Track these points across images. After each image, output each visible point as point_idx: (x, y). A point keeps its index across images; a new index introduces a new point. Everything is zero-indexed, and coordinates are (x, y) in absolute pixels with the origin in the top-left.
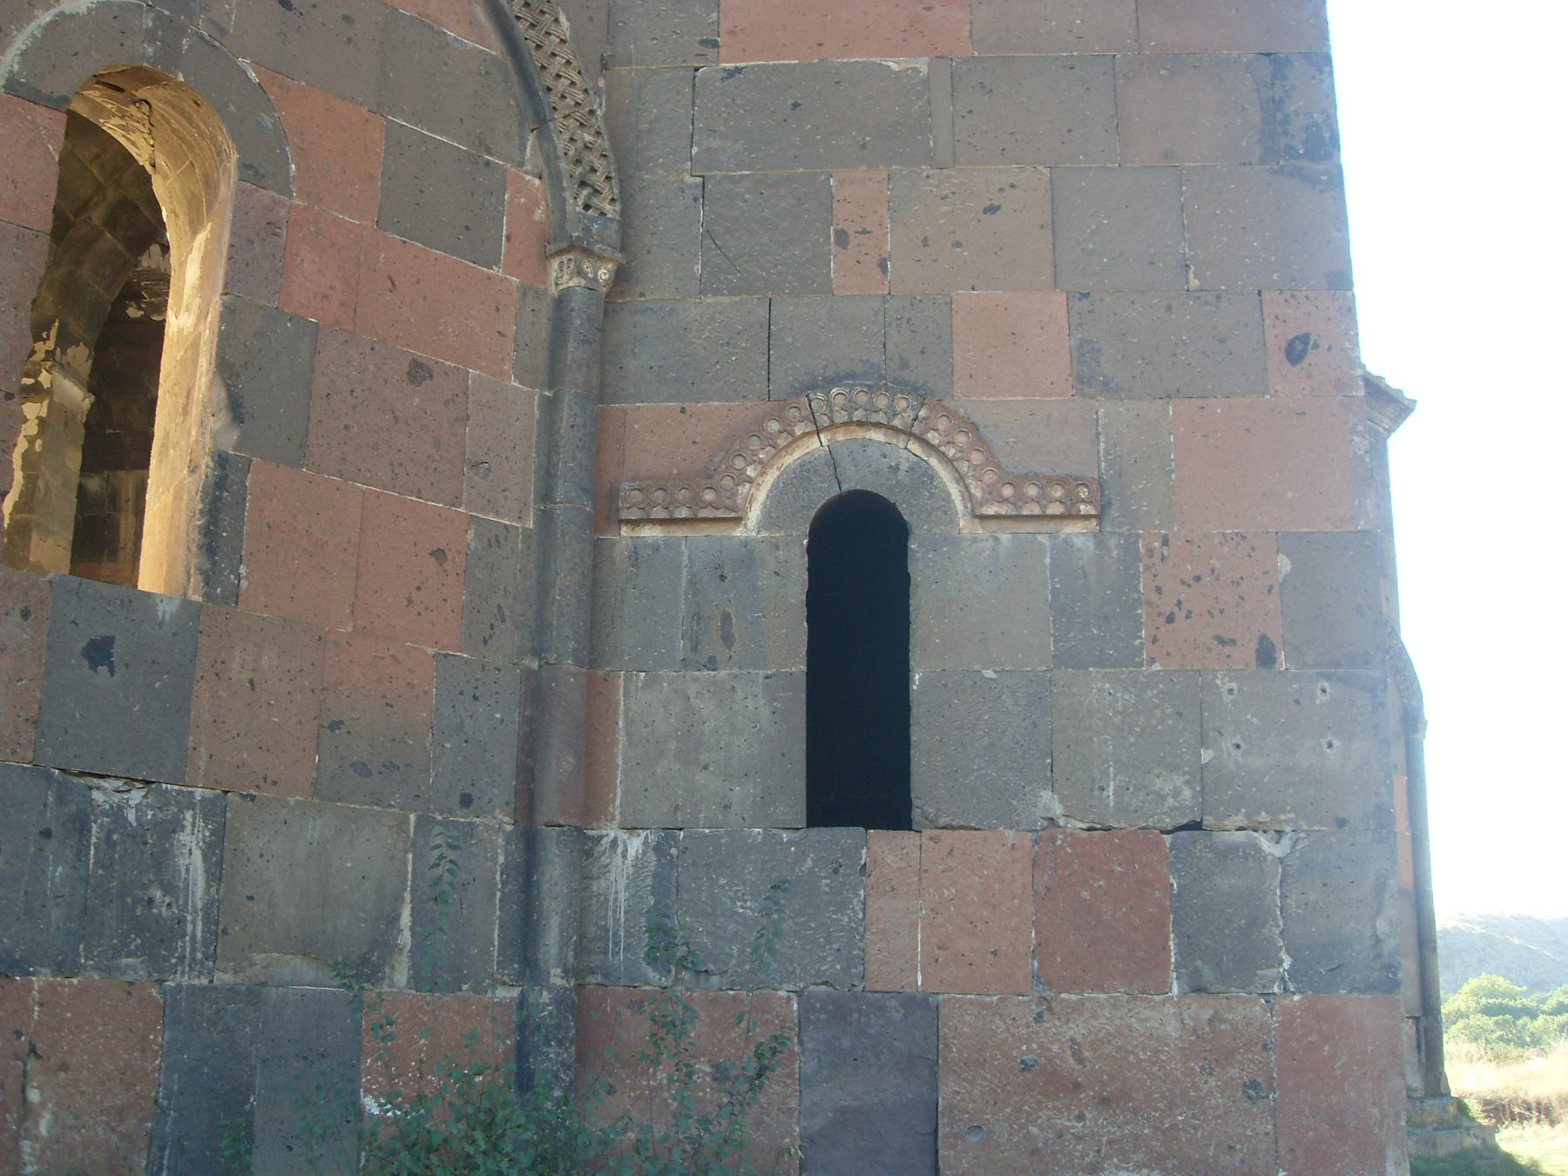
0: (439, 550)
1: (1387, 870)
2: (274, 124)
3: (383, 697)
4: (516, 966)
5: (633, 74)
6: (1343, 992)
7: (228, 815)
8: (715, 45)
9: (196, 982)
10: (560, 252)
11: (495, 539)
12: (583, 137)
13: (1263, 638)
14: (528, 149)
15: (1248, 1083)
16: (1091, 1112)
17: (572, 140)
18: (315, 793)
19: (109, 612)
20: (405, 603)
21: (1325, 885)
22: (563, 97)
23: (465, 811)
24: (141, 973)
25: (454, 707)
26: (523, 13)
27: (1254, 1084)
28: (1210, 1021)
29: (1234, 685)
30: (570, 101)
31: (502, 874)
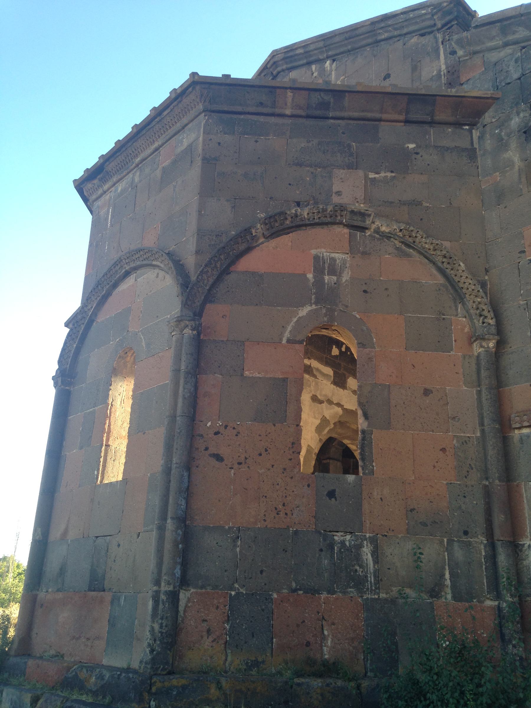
0: (443, 448)
2: (367, 329)
3: (429, 499)
4: (495, 593)
5: (497, 271)
7: (378, 542)
8: (524, 252)
9: (373, 597)
10: (475, 341)
11: (465, 442)
12: (477, 301)
14: (459, 309)
17: (474, 302)
18: (408, 533)
19: (333, 482)
22: (468, 289)
24: (355, 594)
25: (456, 500)
26: (448, 266)
30: (470, 290)
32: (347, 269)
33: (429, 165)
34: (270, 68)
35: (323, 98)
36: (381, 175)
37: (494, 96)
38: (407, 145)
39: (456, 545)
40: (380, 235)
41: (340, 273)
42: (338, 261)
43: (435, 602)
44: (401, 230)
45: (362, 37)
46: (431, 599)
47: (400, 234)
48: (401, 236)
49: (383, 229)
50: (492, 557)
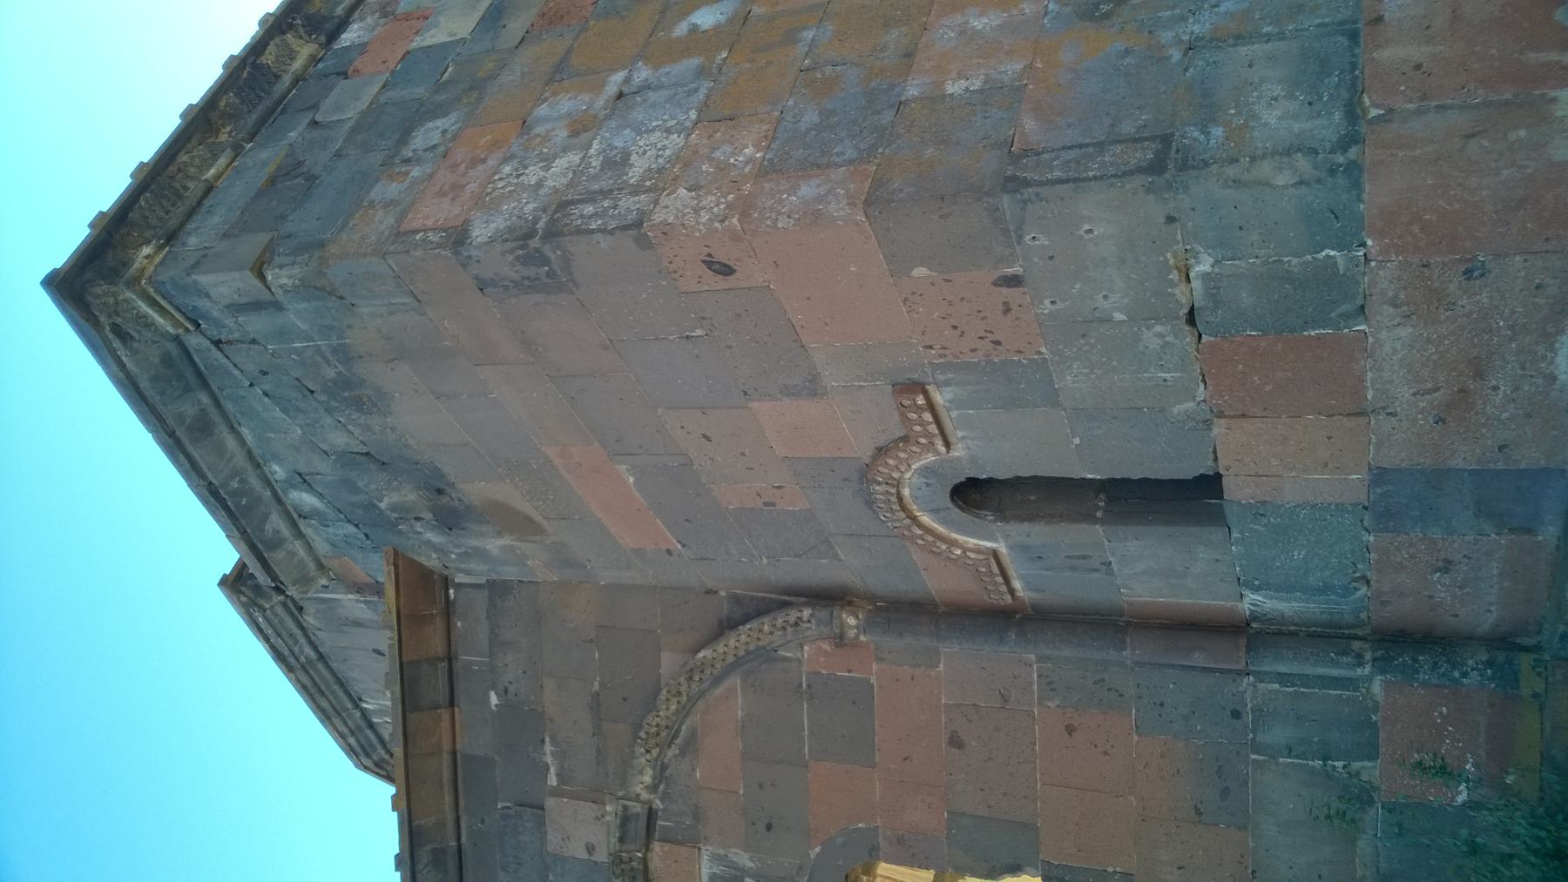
0: (1066, 730)
1: (1218, 181)
2: (840, 837)
6: (1362, 206)
13: (995, 284)
15: (1466, 277)
16: (1495, 401)
18: (1245, 828)
20: (1107, 757)
21: (1241, 228)
23: (1244, 715)
26: (708, 672)
27: (1468, 274)
28: (1395, 306)
29: (1047, 302)
31: (1287, 687)
32: (730, 855)
33: (524, 672)
34: (385, 770)
35: (426, 865)
36: (549, 762)
37: (392, 560)
38: (494, 708)
39: (1262, 738)
40: (660, 782)
41: (737, 869)
42: (715, 870)
43: (1382, 798)
44: (648, 751)
45: (315, 677)
46: (1376, 805)
47: (655, 752)
48: (658, 750)
49: (647, 779)
50: (1283, 679)
